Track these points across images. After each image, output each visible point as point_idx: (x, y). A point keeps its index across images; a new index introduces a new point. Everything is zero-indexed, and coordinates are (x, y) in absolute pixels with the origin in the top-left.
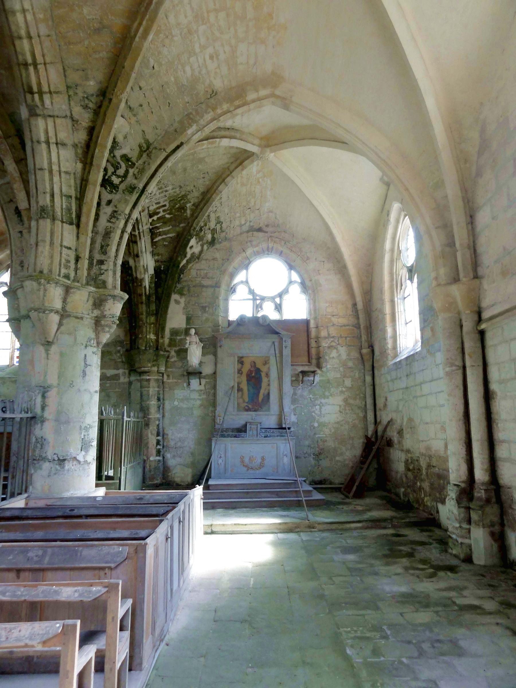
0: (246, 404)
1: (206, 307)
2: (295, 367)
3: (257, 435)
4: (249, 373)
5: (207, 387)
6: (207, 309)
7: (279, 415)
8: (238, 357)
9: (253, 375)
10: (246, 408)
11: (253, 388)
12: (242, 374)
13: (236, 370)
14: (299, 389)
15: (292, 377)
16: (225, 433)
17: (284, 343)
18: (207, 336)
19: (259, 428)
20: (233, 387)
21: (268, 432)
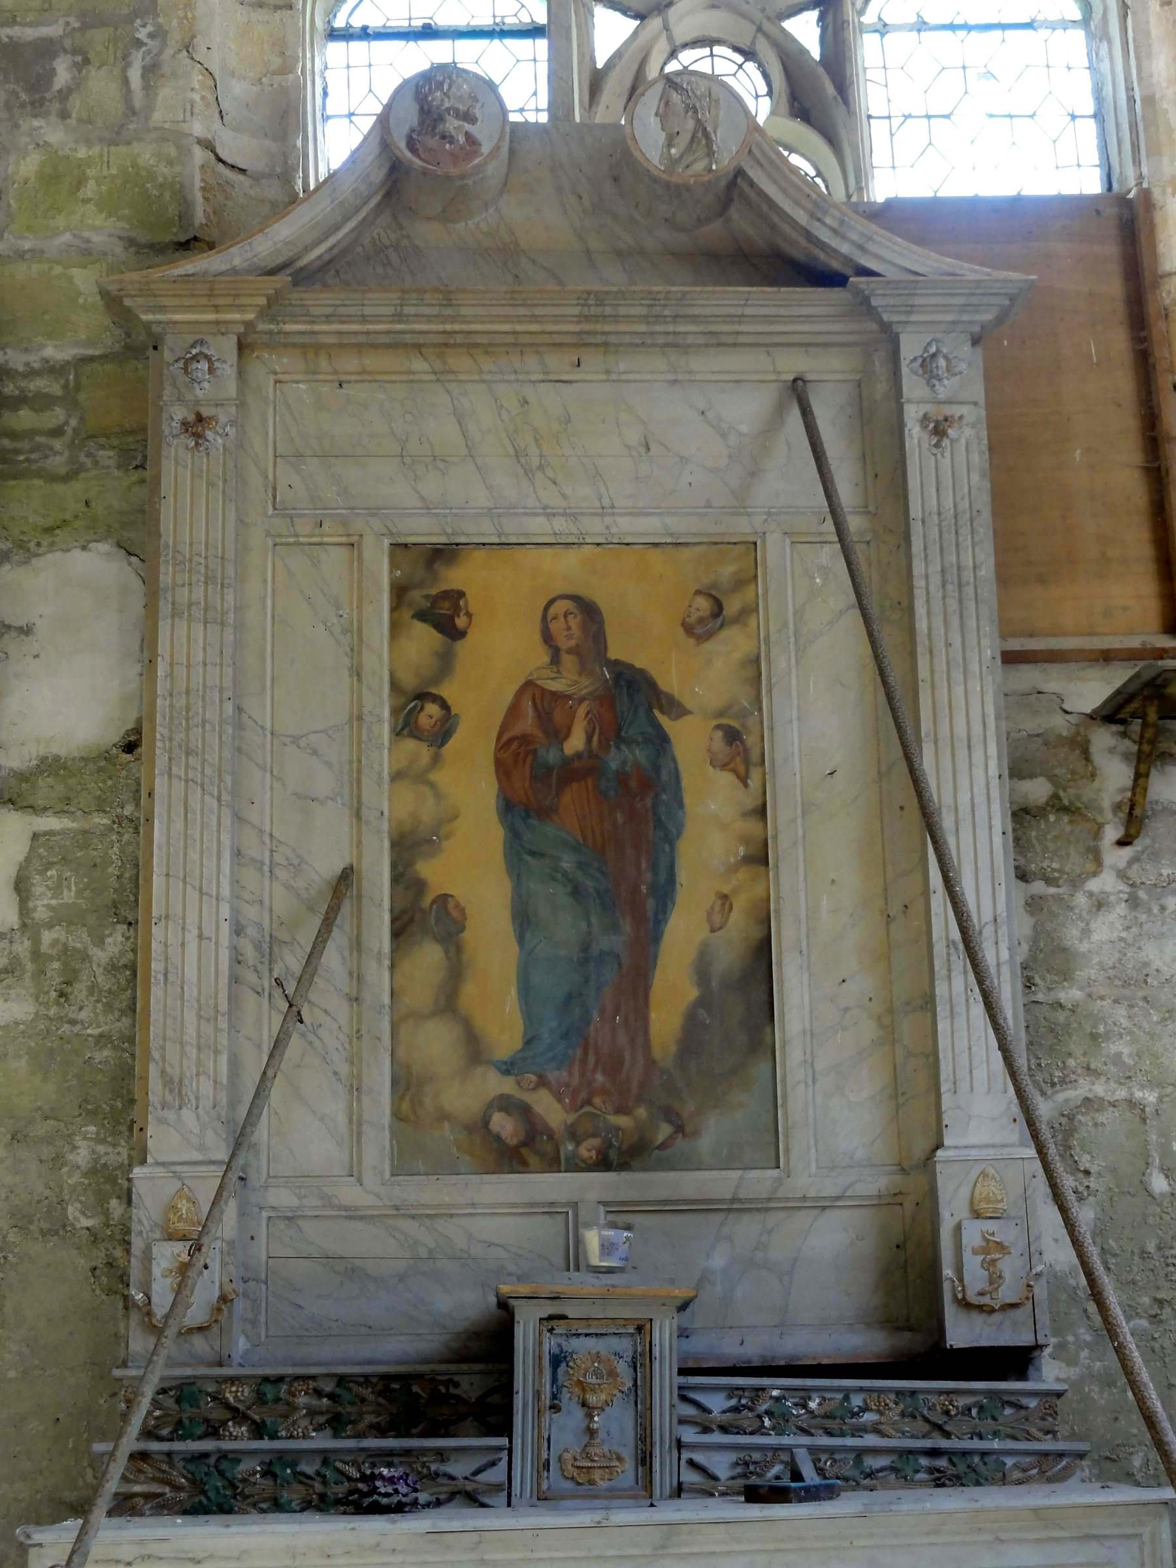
0: (507, 1086)
1: (47, 49)
2: (1028, 677)
3: (645, 1459)
4: (527, 723)
5: (42, 905)
6: (63, 72)
7: (891, 1200)
8: (399, 548)
9: (576, 743)
10: (504, 1125)
11: (576, 892)
12: (442, 734)
13: (380, 706)
14: (1100, 904)
15: (1018, 770)
16: (238, 1439)
17: (912, 385)
18: (53, 352)
19: (665, 1379)
20: (346, 878)
21: (782, 1422)
